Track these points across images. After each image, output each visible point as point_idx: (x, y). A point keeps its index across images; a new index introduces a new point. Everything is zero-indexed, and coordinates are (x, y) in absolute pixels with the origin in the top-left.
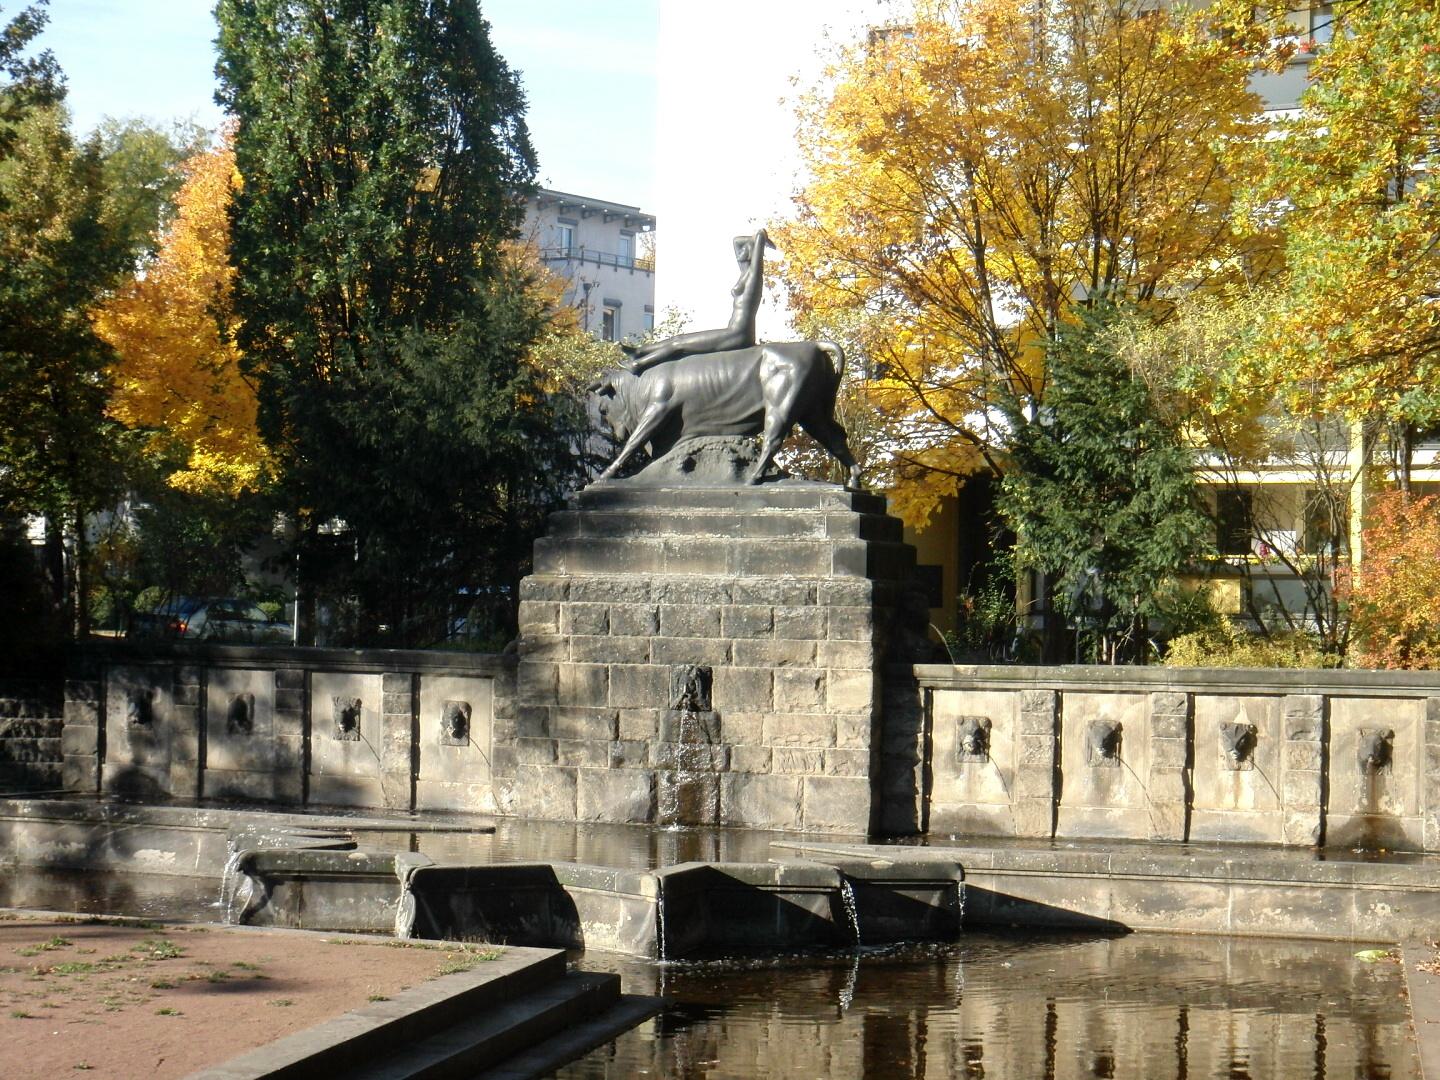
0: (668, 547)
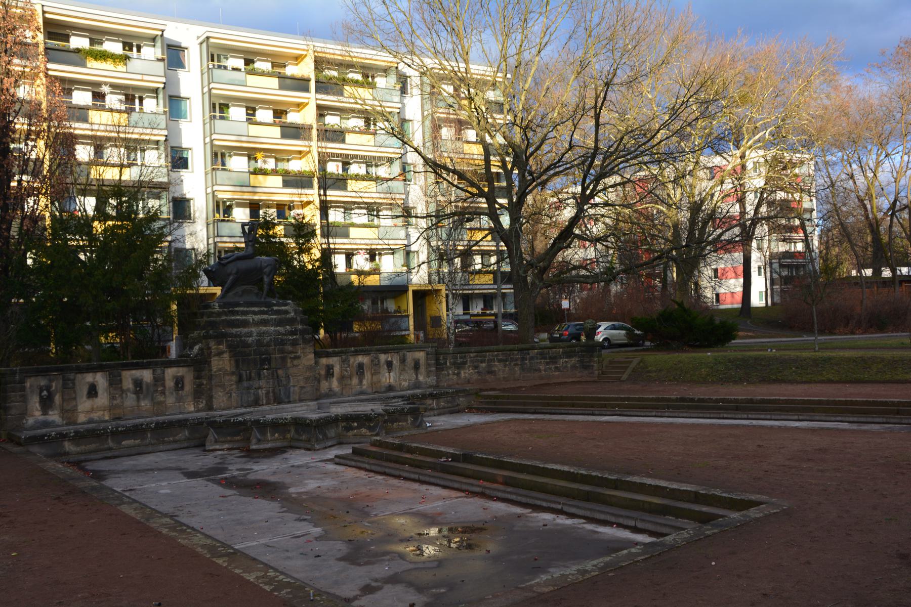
0: (253, 320)
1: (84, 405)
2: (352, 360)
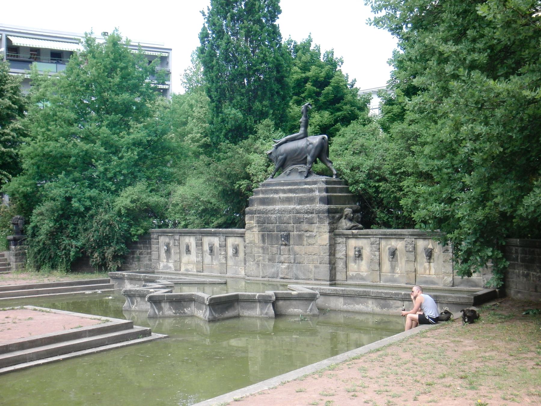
0: (280, 198)
1: (185, 258)
2: (383, 243)
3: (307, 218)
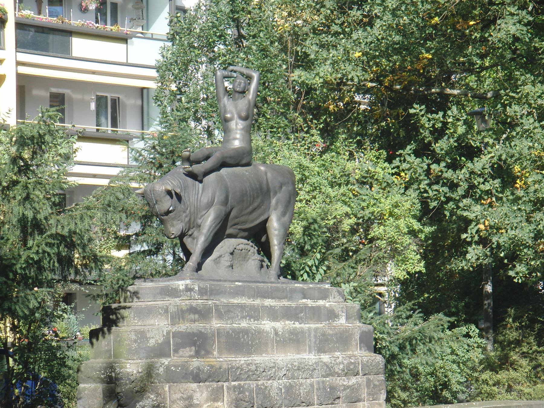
3: (346, 388)
